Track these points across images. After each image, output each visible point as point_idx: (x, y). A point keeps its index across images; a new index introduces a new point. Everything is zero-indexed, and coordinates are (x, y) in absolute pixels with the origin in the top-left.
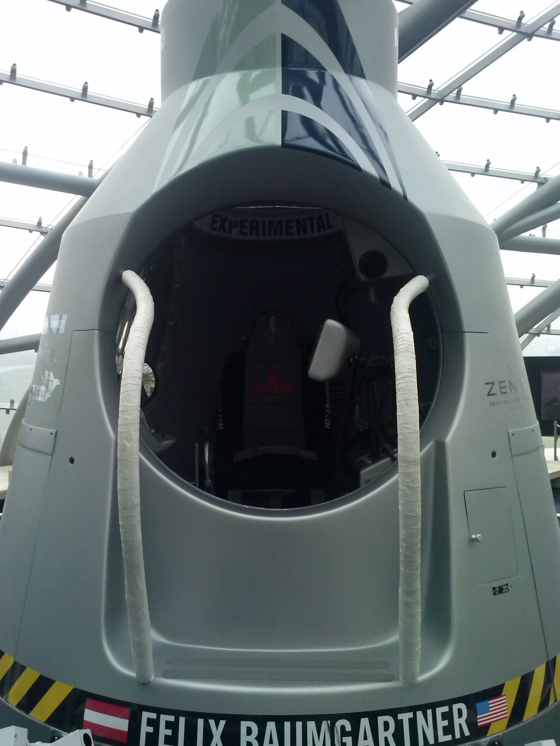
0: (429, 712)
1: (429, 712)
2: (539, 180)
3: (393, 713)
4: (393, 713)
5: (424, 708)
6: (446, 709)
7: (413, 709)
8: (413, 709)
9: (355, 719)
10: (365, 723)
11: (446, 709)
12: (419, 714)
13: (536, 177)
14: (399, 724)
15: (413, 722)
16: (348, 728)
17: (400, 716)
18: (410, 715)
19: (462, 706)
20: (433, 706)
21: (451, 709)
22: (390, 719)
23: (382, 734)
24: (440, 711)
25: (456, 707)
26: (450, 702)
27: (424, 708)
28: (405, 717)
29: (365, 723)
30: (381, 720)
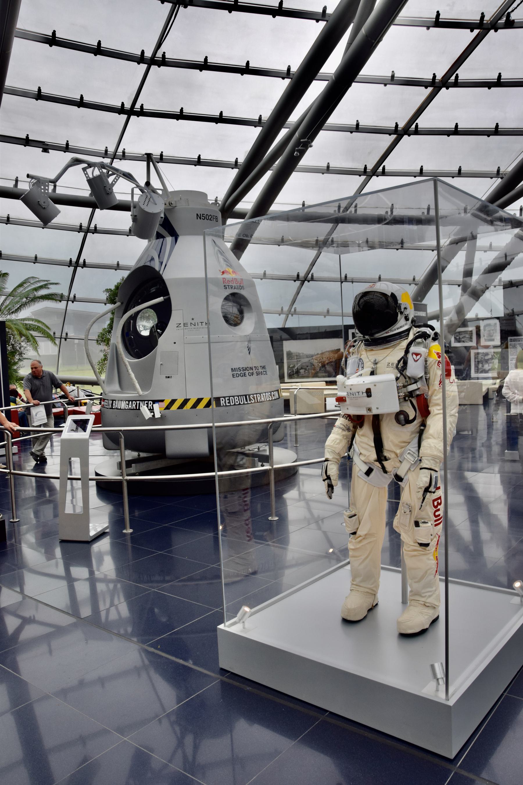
0: (143, 402)
1: (143, 402)
2: (501, 176)
3: (136, 401)
4: (136, 401)
5: (142, 401)
6: (147, 402)
7: (140, 401)
8: (140, 401)
9: (129, 401)
10: (131, 402)
11: (147, 402)
12: (141, 402)
13: (498, 173)
14: (137, 403)
15: (139, 403)
16: (128, 403)
17: (137, 402)
18: (139, 402)
19: (152, 402)
20: (144, 401)
21: (148, 402)
22: (135, 402)
23: (133, 405)
24: (146, 402)
25: (150, 402)
26: (148, 401)
27: (142, 401)
28: (138, 402)
29: (131, 402)
30: (133, 402)
